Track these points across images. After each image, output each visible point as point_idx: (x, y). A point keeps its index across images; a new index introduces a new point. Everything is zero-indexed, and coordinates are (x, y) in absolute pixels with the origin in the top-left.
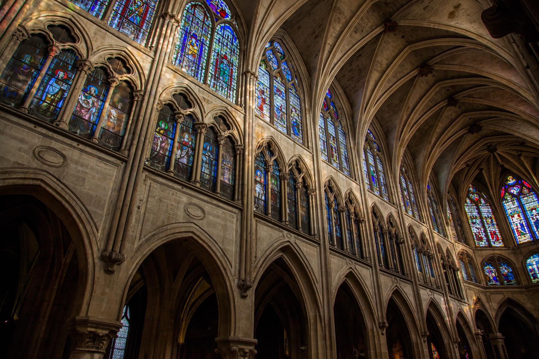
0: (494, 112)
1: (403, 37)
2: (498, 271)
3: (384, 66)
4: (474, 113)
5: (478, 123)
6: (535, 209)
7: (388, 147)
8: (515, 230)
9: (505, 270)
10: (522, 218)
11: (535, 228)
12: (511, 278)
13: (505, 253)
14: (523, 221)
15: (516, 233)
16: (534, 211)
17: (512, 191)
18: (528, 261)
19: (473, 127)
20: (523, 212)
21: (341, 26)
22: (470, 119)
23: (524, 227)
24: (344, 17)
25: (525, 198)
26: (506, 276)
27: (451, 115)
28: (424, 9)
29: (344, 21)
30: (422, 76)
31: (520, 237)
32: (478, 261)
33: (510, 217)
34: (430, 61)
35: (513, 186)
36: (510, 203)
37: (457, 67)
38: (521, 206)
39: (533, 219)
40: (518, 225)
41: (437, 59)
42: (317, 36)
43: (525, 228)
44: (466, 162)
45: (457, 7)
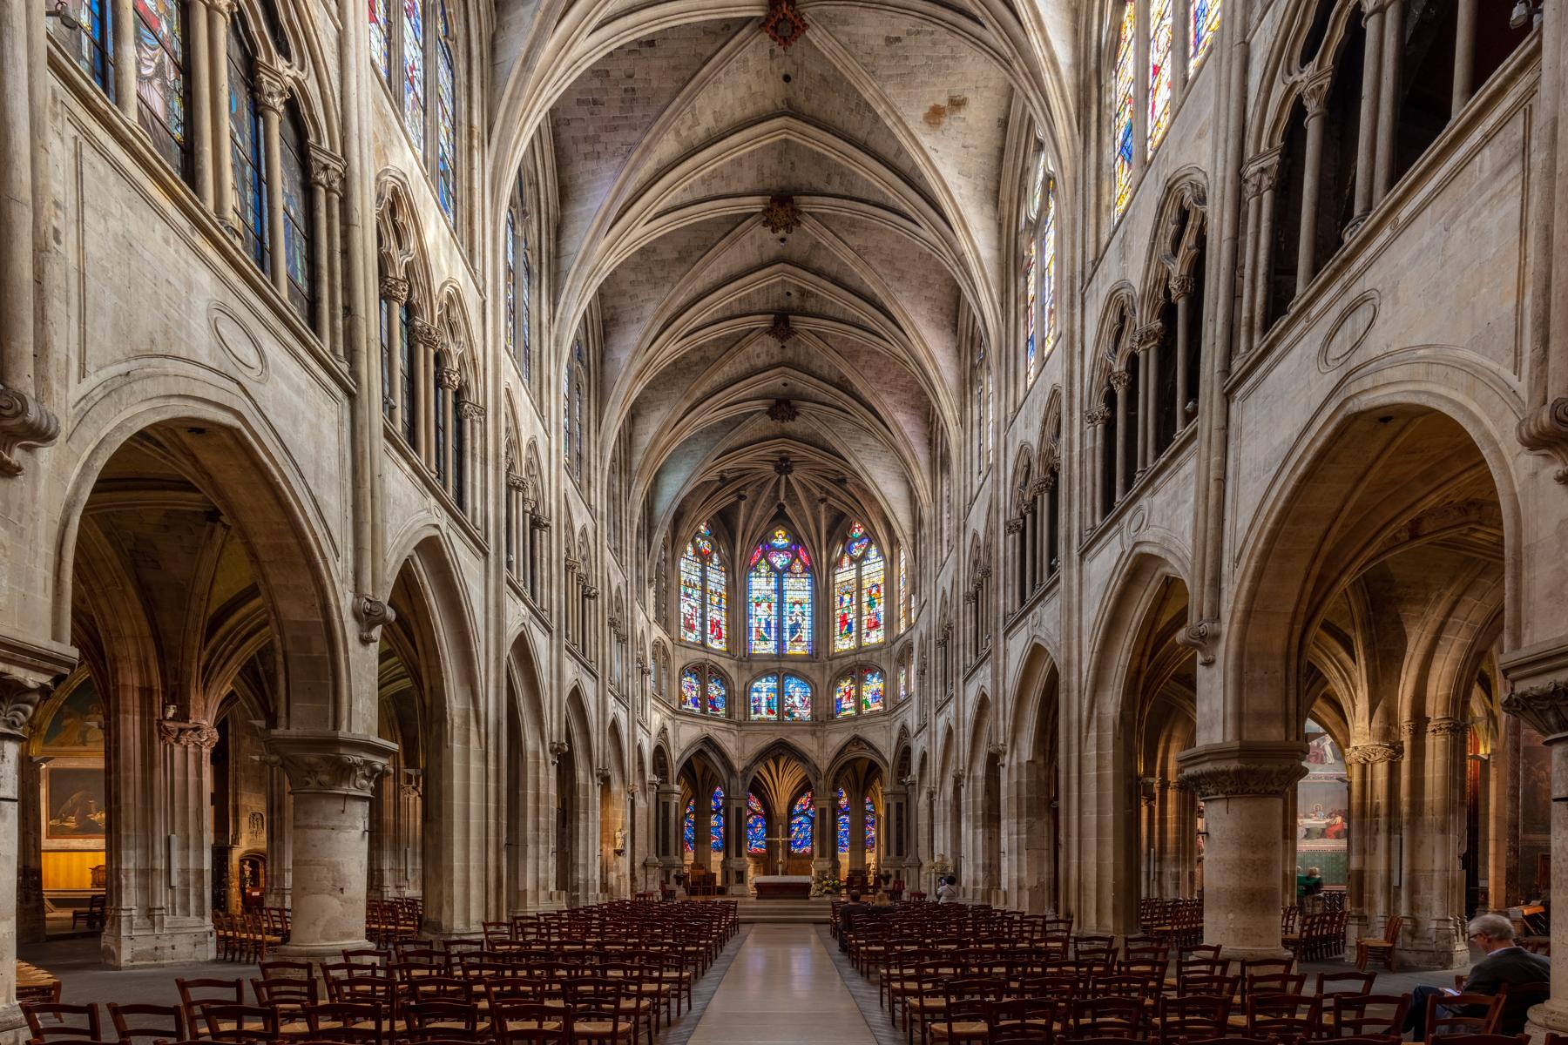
0: (845, 396)
2: (704, 689)
3: (700, 131)
4: (806, 377)
5: (794, 403)
7: (602, 362)
9: (715, 690)
12: (719, 705)
13: (724, 663)
18: (757, 684)
19: (783, 406)
26: (713, 700)
32: (678, 664)
34: (805, 199)
37: (852, 255)
41: (824, 205)
45: (957, 103)
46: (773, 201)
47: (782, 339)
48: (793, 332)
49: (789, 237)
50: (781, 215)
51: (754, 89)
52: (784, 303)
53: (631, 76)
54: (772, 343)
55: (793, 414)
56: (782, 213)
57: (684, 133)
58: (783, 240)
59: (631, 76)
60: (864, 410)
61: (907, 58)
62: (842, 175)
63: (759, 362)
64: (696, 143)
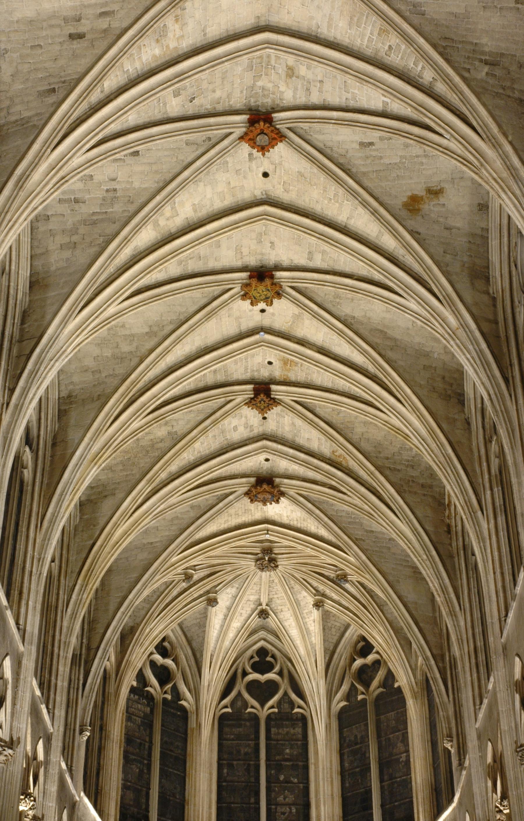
0: (339, 474)
1: (266, 175)
5: (277, 480)
21: (157, 51)
22: (267, 460)
24: (178, 33)
27: (235, 428)
28: (362, 145)
29: (173, 45)
30: (244, 297)
42: (81, 36)
44: (187, 568)
46: (250, 277)
47: (262, 411)
48: (276, 402)
49: (269, 309)
50: (261, 289)
51: (233, 185)
52: (265, 373)
53: (114, 180)
54: (251, 416)
55: (277, 495)
56: (261, 288)
57: (162, 222)
58: (263, 311)
59: (114, 180)
60: (363, 490)
61: (381, 158)
62: (324, 252)
63: (236, 437)
64: (173, 230)
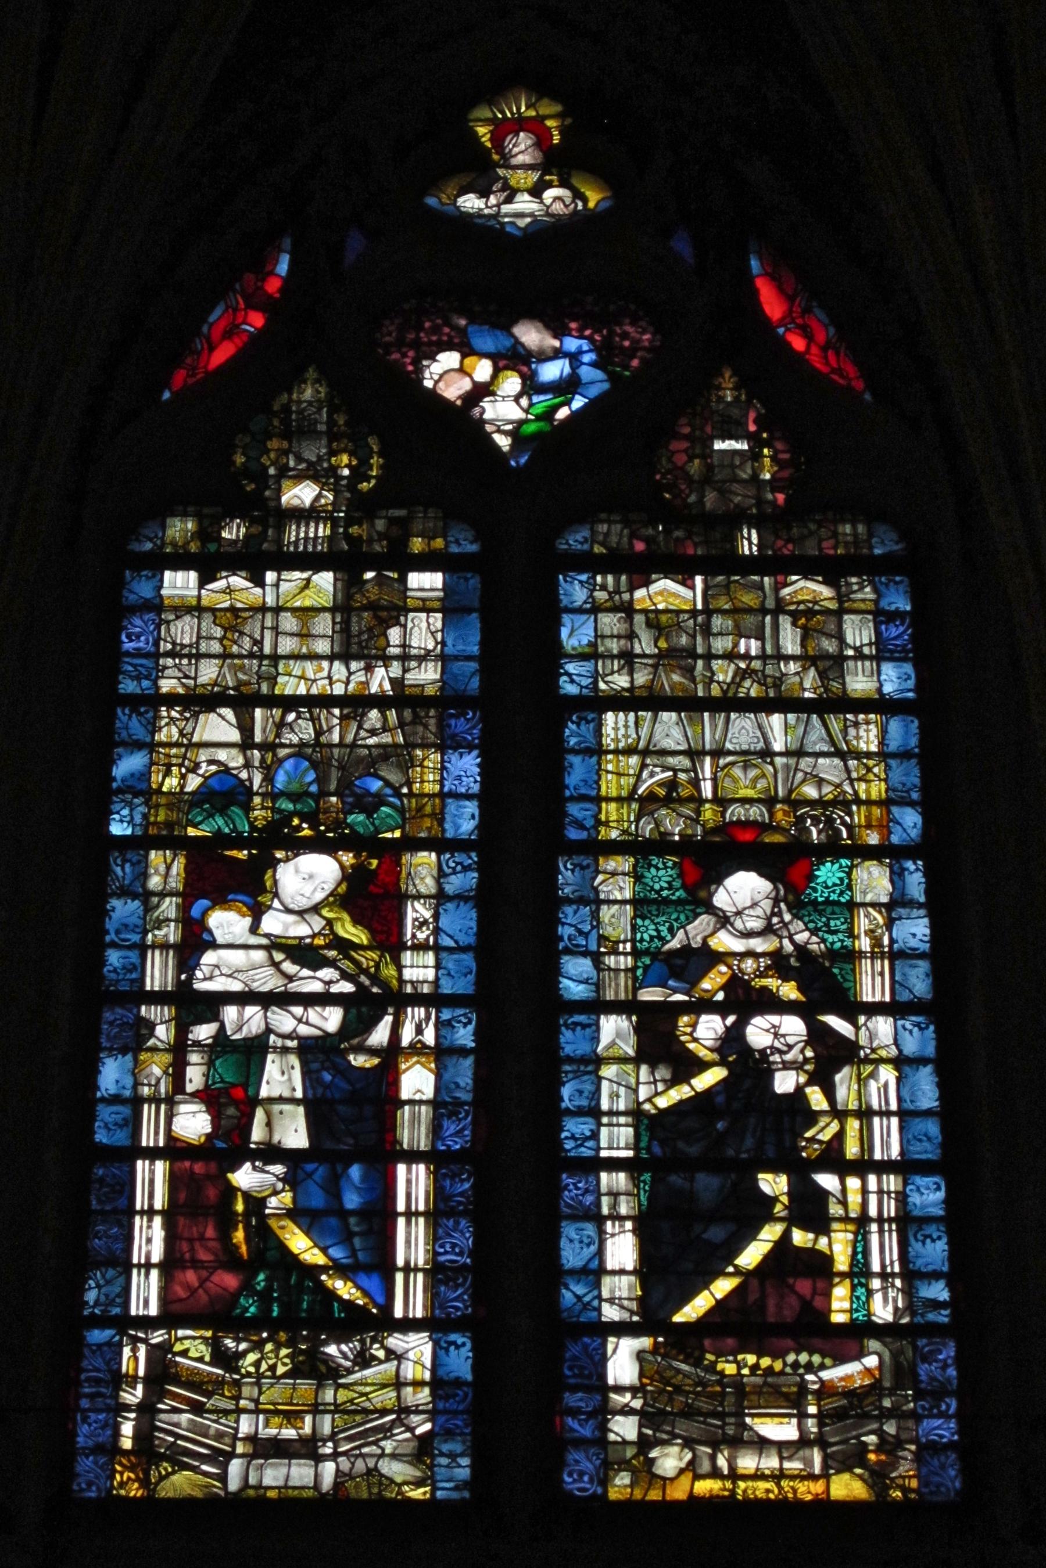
6: (787, 864)
8: (152, 1182)
10: (419, 970)
11: (622, 1250)
14: (417, 1026)
15: (150, 1240)
16: (744, 889)
17: (446, 373)
20: (486, 845)
23: (385, 1156)
25: (665, 592)
31: (193, 1347)
33: (165, 870)
35: (504, 283)
36: (286, 584)
38: (517, 712)
39: (660, 1045)
40: (281, 1077)
43: (412, 1184)
